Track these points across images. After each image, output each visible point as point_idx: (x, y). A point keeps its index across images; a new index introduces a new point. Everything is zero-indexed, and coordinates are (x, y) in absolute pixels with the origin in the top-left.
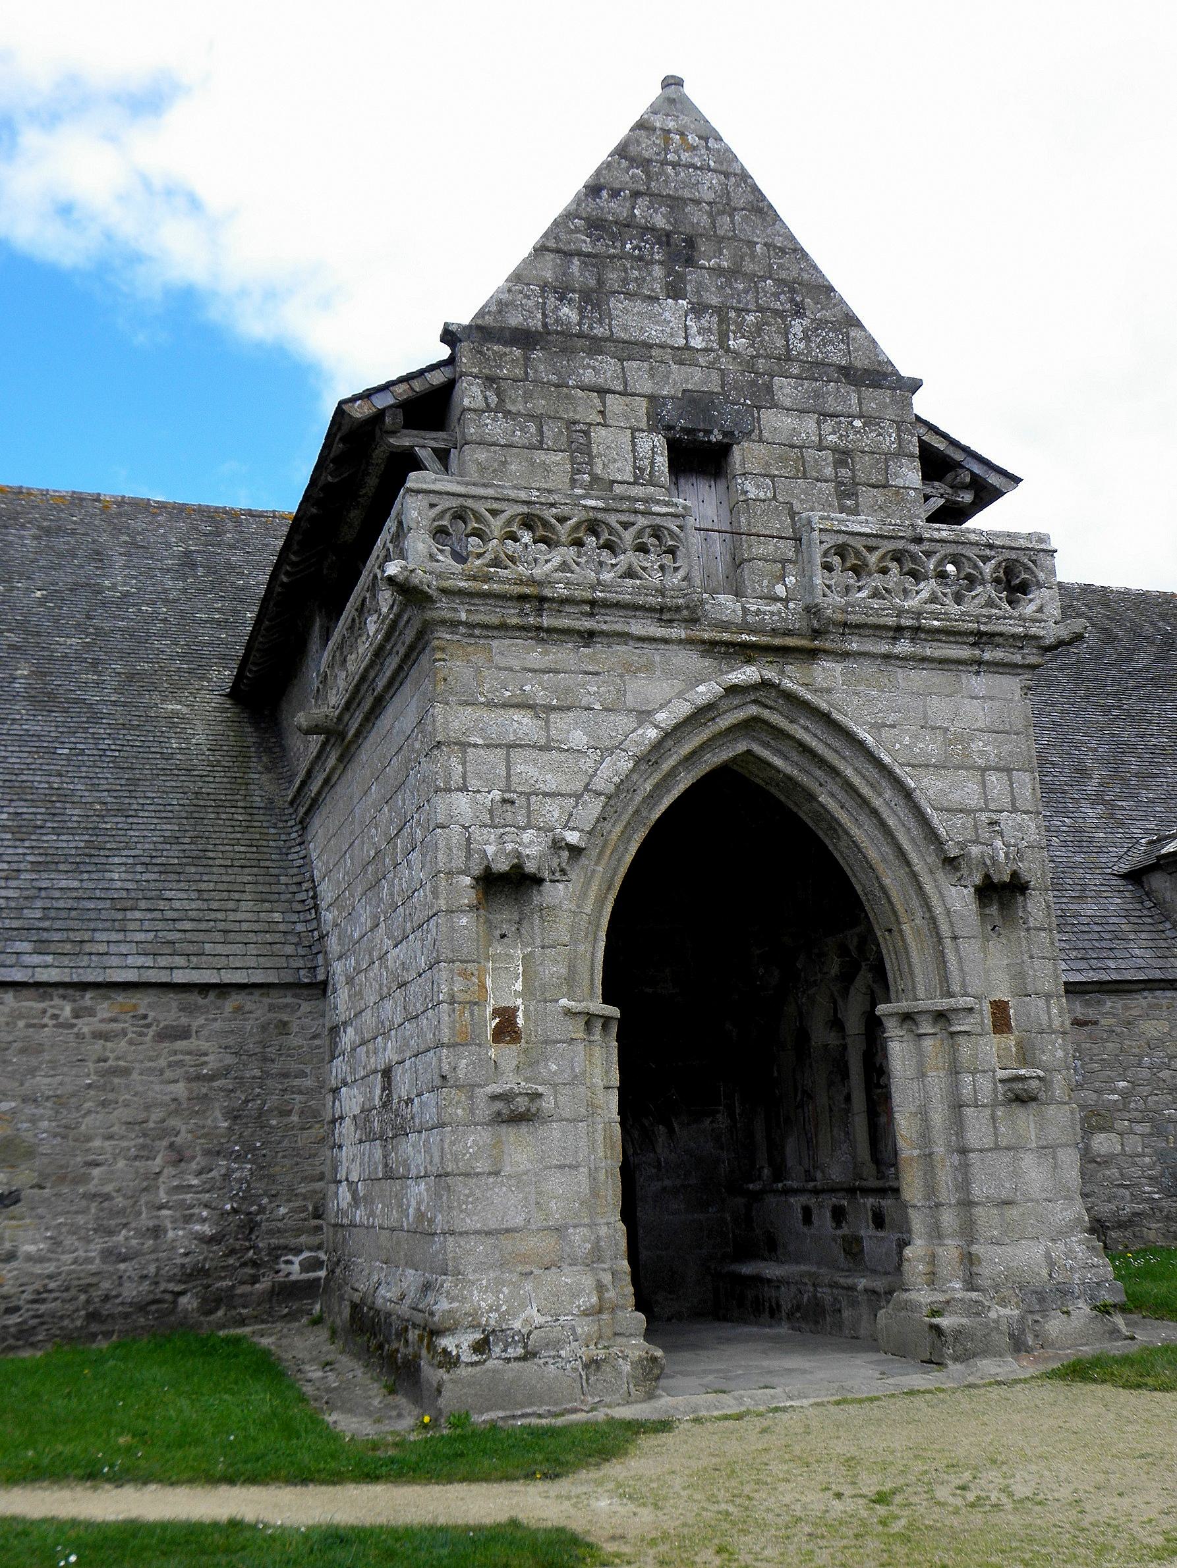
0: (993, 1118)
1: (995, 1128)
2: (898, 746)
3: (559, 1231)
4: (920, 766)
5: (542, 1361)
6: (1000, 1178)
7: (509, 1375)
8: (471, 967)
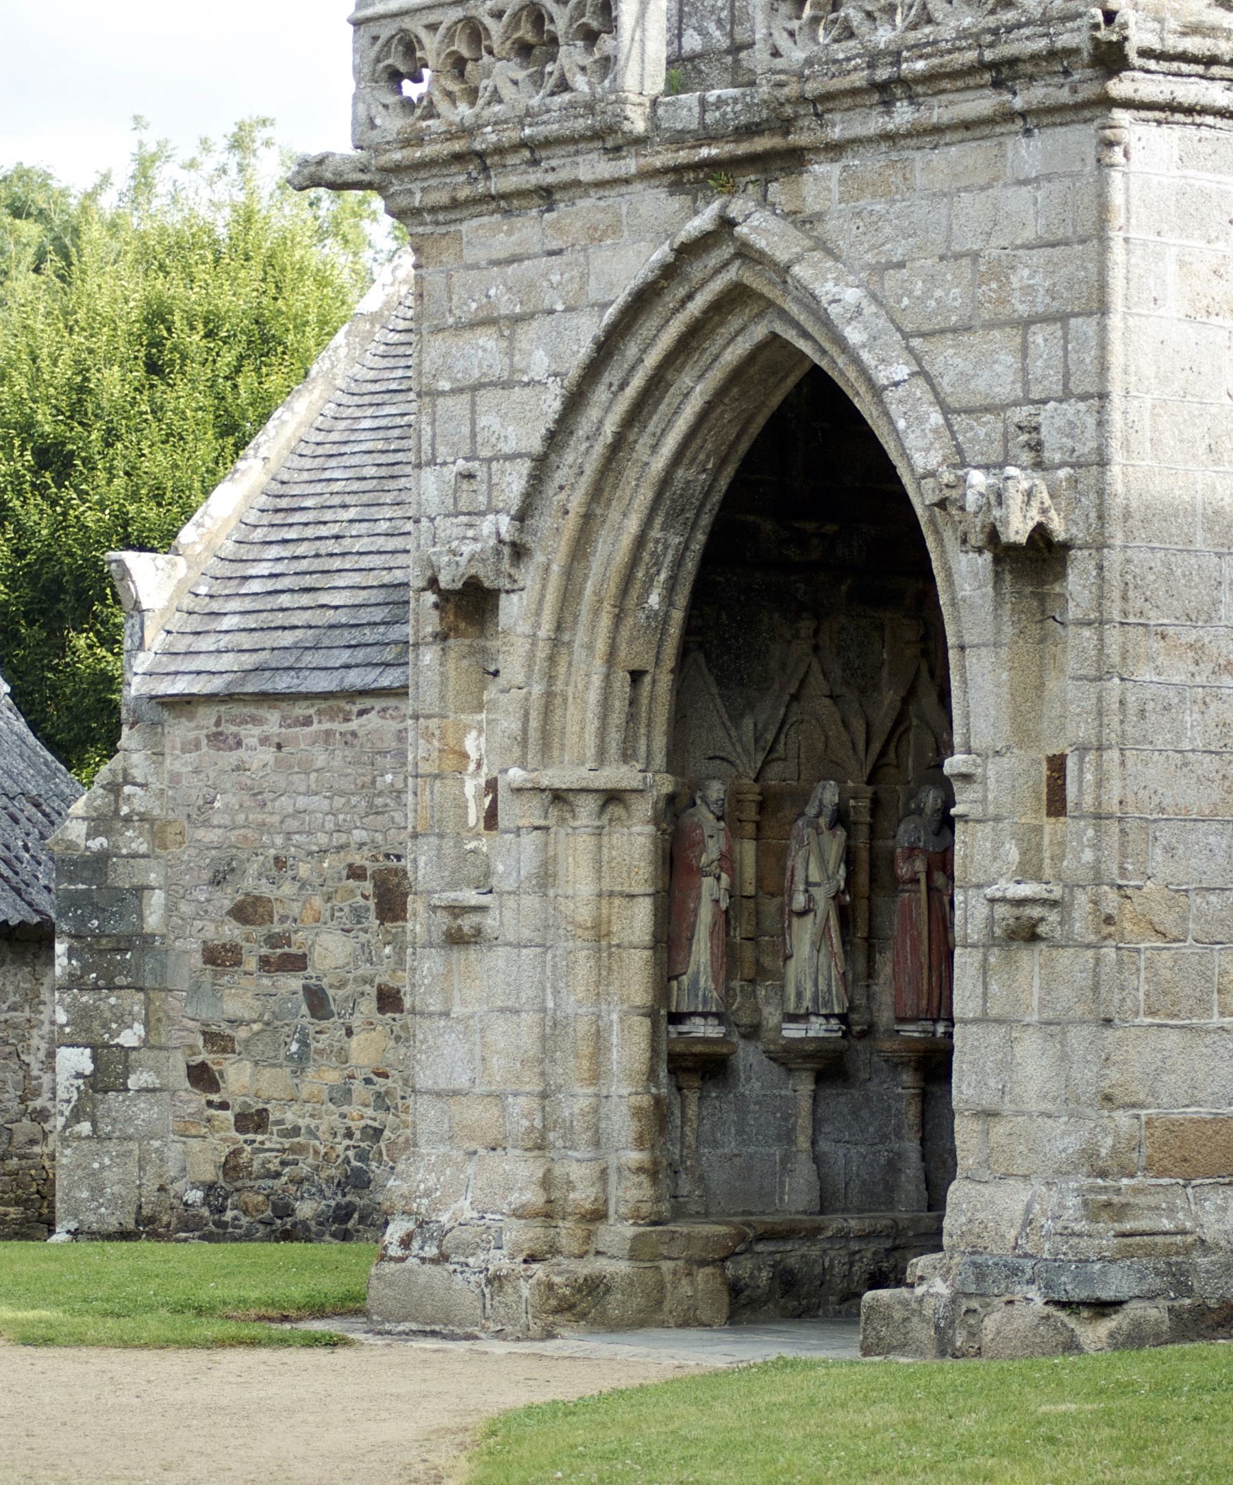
0: (985, 967)
1: (985, 985)
2: (906, 301)
3: (499, 1097)
4: (932, 334)
5: (451, 1268)
6: (983, 1071)
7: (422, 1279)
8: (433, 723)
